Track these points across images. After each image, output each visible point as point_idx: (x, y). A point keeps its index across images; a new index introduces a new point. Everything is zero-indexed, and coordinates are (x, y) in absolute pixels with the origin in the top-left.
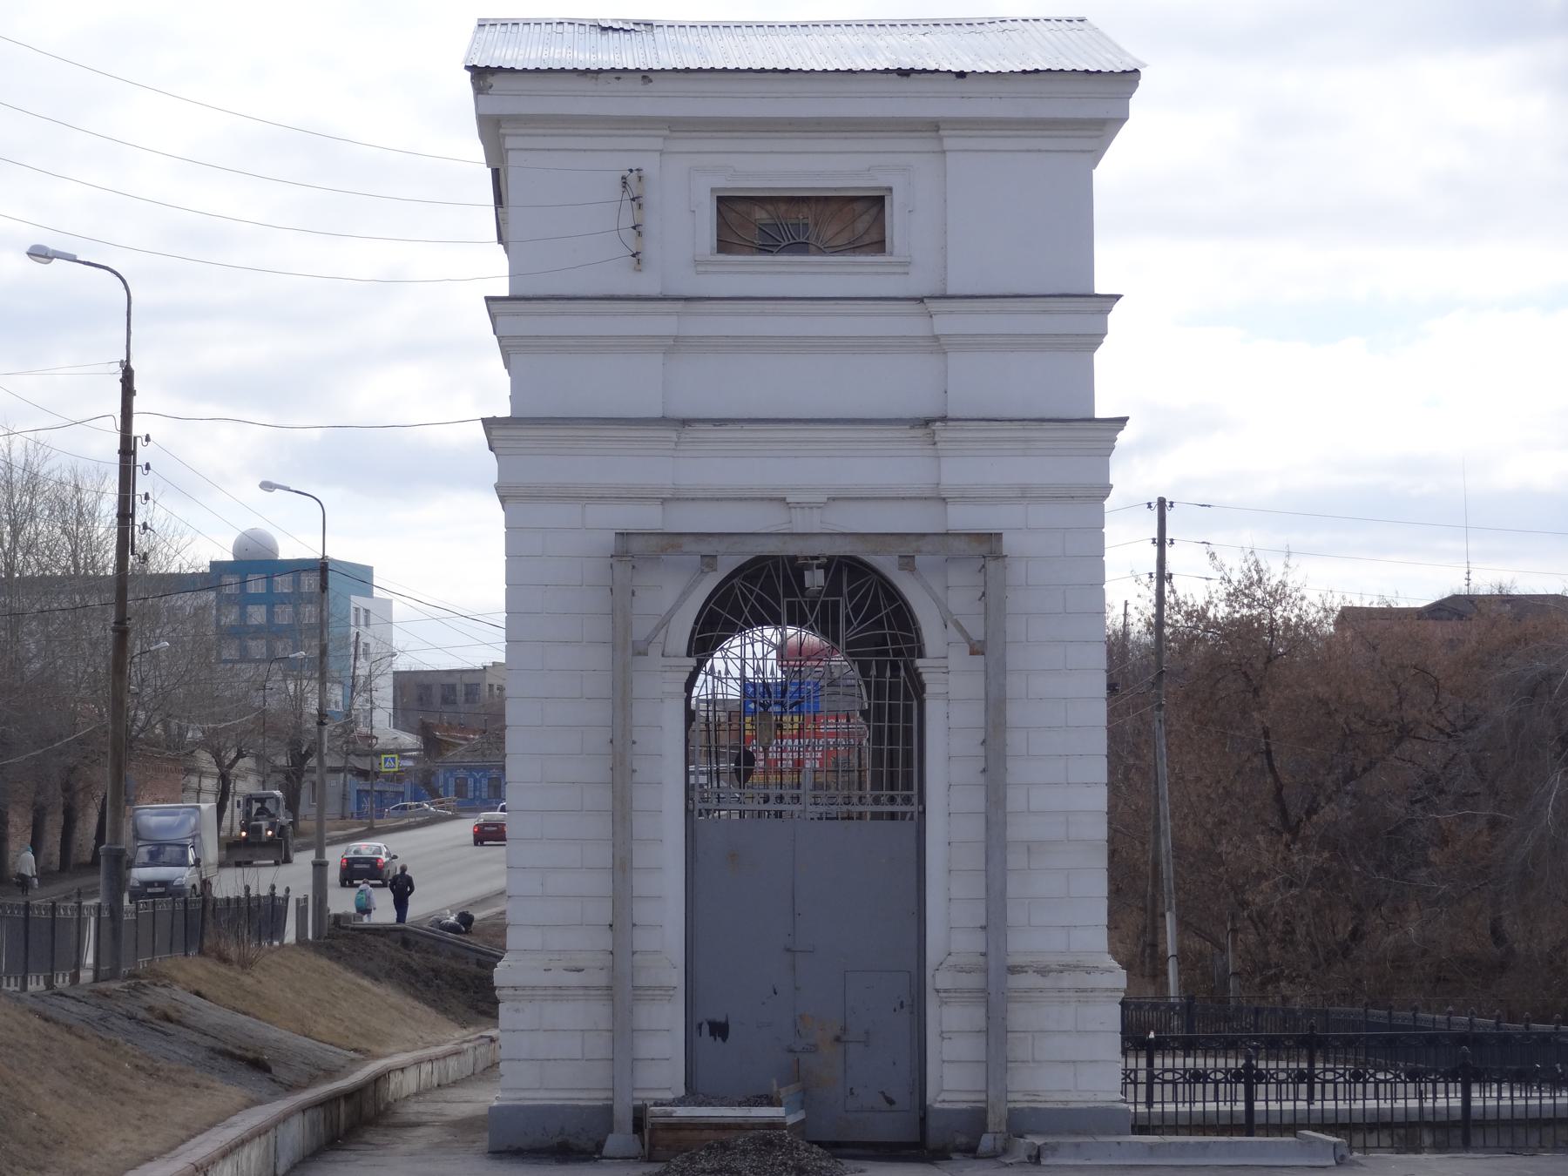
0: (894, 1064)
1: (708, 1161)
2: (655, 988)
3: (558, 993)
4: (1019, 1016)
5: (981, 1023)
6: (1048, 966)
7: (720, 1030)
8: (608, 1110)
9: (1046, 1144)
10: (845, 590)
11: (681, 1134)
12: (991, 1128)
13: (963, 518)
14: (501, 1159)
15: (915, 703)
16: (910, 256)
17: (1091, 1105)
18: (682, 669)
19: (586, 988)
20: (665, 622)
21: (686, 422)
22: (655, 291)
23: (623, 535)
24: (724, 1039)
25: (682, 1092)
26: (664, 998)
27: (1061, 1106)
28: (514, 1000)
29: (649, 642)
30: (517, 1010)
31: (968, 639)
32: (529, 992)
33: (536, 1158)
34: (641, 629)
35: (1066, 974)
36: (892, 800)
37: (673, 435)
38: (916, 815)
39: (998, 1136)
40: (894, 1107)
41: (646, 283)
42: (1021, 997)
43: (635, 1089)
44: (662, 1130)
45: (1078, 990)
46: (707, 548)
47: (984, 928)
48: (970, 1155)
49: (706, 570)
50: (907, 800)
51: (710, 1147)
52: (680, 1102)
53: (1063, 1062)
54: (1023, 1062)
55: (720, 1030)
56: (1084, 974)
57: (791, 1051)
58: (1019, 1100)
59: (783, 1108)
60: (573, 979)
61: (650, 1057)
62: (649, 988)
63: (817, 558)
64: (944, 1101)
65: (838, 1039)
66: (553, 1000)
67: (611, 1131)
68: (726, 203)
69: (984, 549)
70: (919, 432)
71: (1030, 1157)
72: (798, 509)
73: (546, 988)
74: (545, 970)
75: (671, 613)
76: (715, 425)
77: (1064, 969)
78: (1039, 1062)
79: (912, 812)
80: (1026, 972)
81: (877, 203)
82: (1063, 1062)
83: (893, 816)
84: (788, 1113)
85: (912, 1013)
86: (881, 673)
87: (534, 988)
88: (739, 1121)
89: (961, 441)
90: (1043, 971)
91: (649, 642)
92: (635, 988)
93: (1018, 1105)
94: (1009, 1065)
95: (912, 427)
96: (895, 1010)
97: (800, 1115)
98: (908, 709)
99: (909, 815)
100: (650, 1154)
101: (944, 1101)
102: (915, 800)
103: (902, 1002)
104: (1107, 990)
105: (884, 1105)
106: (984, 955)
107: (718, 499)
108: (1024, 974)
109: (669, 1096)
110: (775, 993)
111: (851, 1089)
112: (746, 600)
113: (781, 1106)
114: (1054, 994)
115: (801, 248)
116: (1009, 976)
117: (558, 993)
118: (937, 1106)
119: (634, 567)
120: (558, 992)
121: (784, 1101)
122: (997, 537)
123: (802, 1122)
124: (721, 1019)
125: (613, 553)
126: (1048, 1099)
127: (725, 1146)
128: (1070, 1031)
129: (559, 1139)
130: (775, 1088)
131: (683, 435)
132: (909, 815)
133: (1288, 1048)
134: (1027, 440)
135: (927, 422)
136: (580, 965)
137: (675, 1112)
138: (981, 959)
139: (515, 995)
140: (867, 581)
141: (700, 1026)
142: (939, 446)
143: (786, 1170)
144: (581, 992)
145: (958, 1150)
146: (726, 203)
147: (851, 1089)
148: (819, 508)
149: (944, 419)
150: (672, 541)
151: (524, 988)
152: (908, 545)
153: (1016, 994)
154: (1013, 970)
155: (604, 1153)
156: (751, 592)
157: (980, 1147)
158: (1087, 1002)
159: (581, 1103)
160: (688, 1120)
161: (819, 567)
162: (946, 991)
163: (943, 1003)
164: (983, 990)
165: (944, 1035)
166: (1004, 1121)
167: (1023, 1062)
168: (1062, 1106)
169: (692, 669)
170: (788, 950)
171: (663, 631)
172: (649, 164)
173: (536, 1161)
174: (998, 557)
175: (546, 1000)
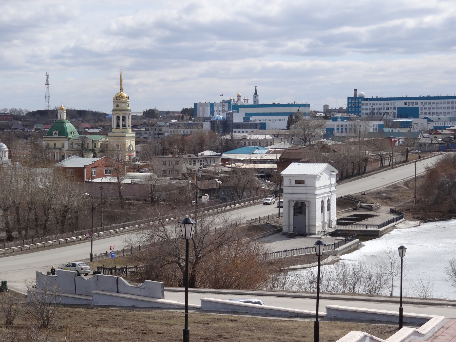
3: (286, 225)
4: (310, 228)
7: (295, 228)
13: (308, 200)
34: (290, 205)
52: (292, 232)
55: (295, 228)
115: (300, 183)
117: (286, 225)
149: (307, 194)
150: (292, 201)
152: (306, 201)
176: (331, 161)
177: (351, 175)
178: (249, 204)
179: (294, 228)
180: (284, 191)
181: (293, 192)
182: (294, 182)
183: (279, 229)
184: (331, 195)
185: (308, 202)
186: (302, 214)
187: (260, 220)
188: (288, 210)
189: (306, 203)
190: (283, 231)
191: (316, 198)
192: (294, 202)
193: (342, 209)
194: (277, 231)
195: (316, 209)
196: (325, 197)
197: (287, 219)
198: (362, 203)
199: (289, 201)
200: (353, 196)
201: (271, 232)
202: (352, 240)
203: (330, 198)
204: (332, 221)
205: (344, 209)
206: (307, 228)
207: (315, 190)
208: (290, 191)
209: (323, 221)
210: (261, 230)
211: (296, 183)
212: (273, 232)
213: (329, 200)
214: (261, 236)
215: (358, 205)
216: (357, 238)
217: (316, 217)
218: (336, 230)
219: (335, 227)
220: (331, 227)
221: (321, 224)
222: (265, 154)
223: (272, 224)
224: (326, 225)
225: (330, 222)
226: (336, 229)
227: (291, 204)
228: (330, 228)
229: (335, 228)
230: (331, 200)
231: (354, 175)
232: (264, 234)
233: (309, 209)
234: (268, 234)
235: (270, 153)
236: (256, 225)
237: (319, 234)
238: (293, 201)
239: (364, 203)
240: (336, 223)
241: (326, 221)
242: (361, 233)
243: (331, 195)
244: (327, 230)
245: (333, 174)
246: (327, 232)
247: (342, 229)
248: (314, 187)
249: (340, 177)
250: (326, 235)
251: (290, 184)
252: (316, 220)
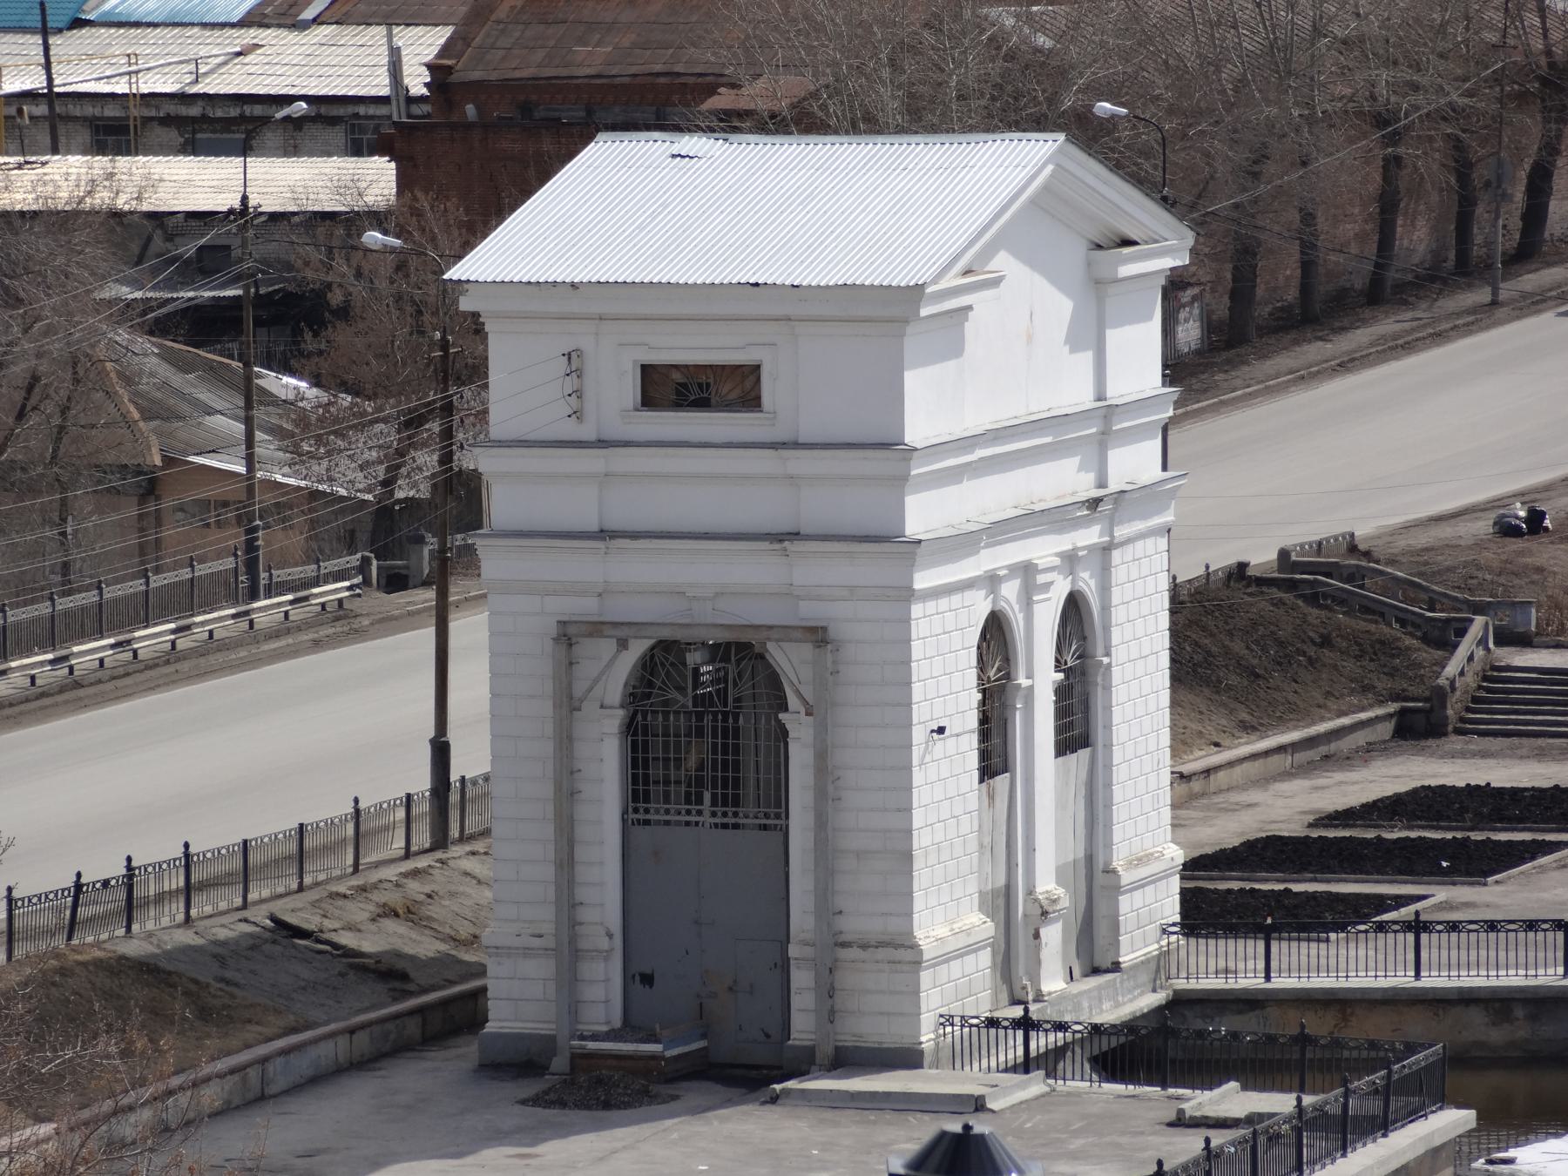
2: (593, 951)
3: (527, 952)
4: (847, 979)
7: (648, 980)
12: (817, 1061)
13: (810, 612)
16: (775, 413)
19: (546, 949)
22: (592, 437)
23: (563, 624)
24: (651, 987)
27: (876, 1046)
30: (499, 964)
34: (579, 689)
41: (587, 432)
46: (620, 633)
50: (778, 816)
52: (611, 1035)
55: (648, 980)
58: (848, 1041)
60: (537, 942)
62: (588, 951)
65: (730, 989)
67: (555, 1055)
68: (647, 371)
73: (517, 948)
77: (881, 944)
81: (756, 369)
84: (665, 1049)
87: (509, 948)
90: (864, 946)
93: (846, 1044)
102: (783, 815)
103: (776, 964)
112: (662, 664)
113: (660, 1043)
115: (702, 404)
117: (527, 952)
120: (527, 951)
122: (824, 629)
123: (704, 1048)
124: (648, 971)
133: (1395, 932)
140: (747, 654)
141: (634, 976)
146: (647, 371)
149: (795, 535)
150: (596, 628)
151: (503, 948)
154: (844, 945)
156: (667, 659)
159: (543, 1032)
172: (586, 343)
176: (1105, 107)
177: (1359, 283)
178: (47, 676)
179: (639, 979)
180: (501, 505)
181: (615, 521)
182: (630, 389)
183: (445, 1003)
184: (1106, 549)
185: (806, 651)
186: (730, 798)
187: (188, 890)
188: (549, 748)
189: (789, 660)
190: (490, 1027)
191: (907, 595)
192: (623, 644)
193: (1248, 728)
194: (413, 1028)
195: (919, 735)
196: (1027, 570)
197: (549, 872)
198: (1507, 638)
199: (568, 636)
200: (1392, 562)
201: (343, 1042)
202: (1382, 1125)
203: (1088, 583)
204: (1126, 878)
205: (1281, 723)
206: (801, 979)
207: (899, 482)
208: (581, 510)
209: (1008, 891)
210: (204, 1014)
211: (649, 401)
212: (362, 1038)
213: (1074, 608)
214: (211, 1096)
215: (1451, 669)
216: (1445, 1099)
217: (921, 840)
218: (1181, 1002)
219: (1164, 955)
220: (1116, 967)
221: (981, 925)
222: (242, 24)
223: (347, 939)
224: (1053, 935)
225: (1101, 909)
226: (1181, 984)
227: (587, 670)
228: (1095, 971)
229: (1160, 966)
230: (1106, 608)
231: (1400, 287)
232: (253, 1074)
233: (822, 730)
234: (302, 1065)
235: (309, 14)
236: (134, 948)
237: (957, 1057)
238: (619, 632)
239: (1524, 641)
240: (1171, 910)
241: (1047, 884)
242: (1497, 1036)
243: (1106, 549)
244: (1063, 997)
245: (1126, 270)
246: (1061, 1027)
247: (1249, 980)
248: (890, 445)
249: (1222, 307)
250: (1050, 1062)
251: (577, 414)
252: (923, 876)
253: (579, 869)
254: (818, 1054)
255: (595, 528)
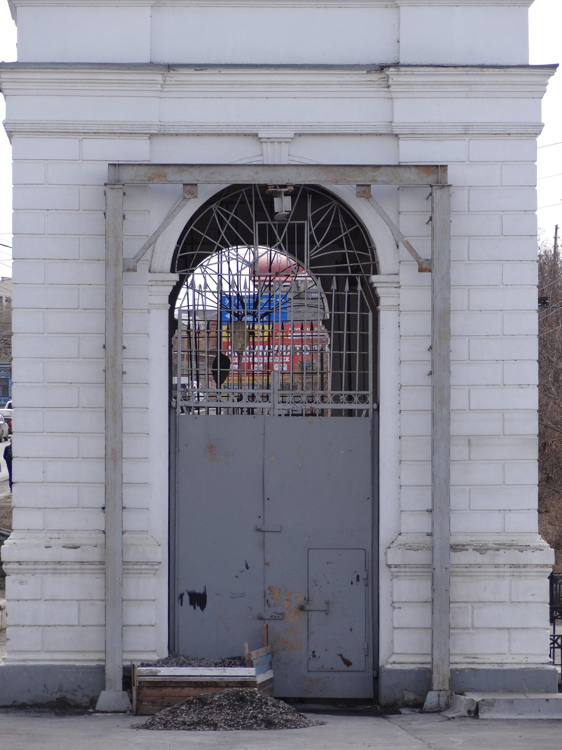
0: (351, 630)
1: (188, 714)
2: (142, 563)
5: (427, 594)
6: (486, 544)
8: (101, 669)
9: (483, 700)
10: (310, 215)
11: (165, 691)
12: (435, 687)
14: (7, 713)
15: (370, 314)
17: (523, 666)
18: (166, 283)
19: (82, 563)
20: (151, 243)
21: (170, 67)
25: (165, 654)
26: (150, 571)
27: (496, 667)
28: (19, 573)
29: (137, 259)
30: (21, 583)
31: (417, 258)
32: (32, 567)
33: (37, 712)
35: (502, 552)
36: (350, 399)
37: (159, 78)
38: (371, 412)
39: (442, 693)
40: (351, 668)
42: (463, 572)
43: (123, 651)
44: (148, 687)
45: (512, 566)
46: (188, 177)
47: (430, 511)
48: (417, 710)
49: (187, 196)
50: (363, 399)
51: (190, 703)
53: (498, 629)
54: (464, 629)
56: (517, 552)
57: (261, 618)
59: (254, 669)
60: (71, 555)
61: (138, 624)
62: (137, 563)
63: (285, 186)
64: (394, 663)
65: (302, 608)
66: (53, 574)
67: (104, 689)
69: (431, 179)
70: (375, 77)
71: (469, 712)
72: (269, 144)
73: (46, 563)
74: (46, 547)
75: (157, 234)
76: (196, 70)
78: (477, 629)
79: (368, 410)
80: (467, 550)
82: (498, 629)
83: (350, 413)
84: (258, 673)
85: (366, 585)
86: (340, 287)
87: (36, 563)
88: (215, 679)
89: (412, 85)
90: (482, 549)
91: (137, 259)
92: (124, 563)
93: (459, 667)
94: (452, 631)
95: (369, 72)
96: (352, 583)
97: (269, 675)
98: (364, 319)
99: (364, 413)
100: (137, 709)
101: (394, 663)
102: (370, 399)
103: (358, 577)
104: (537, 566)
105: (344, 667)
106: (430, 535)
107: (198, 135)
108: (465, 552)
109: (154, 657)
110: (247, 568)
111: (314, 652)
113: (252, 667)
114: (491, 570)
116: (452, 554)
118: (389, 666)
119: (124, 194)
120: (58, 566)
121: (255, 662)
123: (271, 680)
125: (107, 182)
126: (486, 661)
127: (203, 702)
128: (504, 602)
129: (58, 696)
130: (247, 651)
131: (168, 79)
132: (364, 413)
134: (469, 84)
135: (382, 68)
136: (76, 542)
137: (160, 671)
138: (428, 538)
139: (19, 569)
141: (181, 596)
142: (392, 89)
143: (256, 723)
144: (77, 567)
145: (406, 705)
147: (314, 652)
148: (287, 142)
149: (397, 65)
151: (27, 563)
153: (457, 569)
154: (455, 548)
155: (98, 707)
156: (227, 216)
157: (425, 703)
158: (520, 576)
159: (78, 664)
160: (168, 679)
161: (286, 194)
162: (396, 566)
163: (394, 577)
164: (429, 566)
165: (395, 605)
166: (447, 681)
167: (464, 629)
168: (499, 668)
169: (175, 284)
170: (259, 530)
171: (150, 250)
173: (38, 714)
174: (443, 187)
175: (46, 573)
253: (127, 467)
254: (435, 676)
255: (148, 61)
